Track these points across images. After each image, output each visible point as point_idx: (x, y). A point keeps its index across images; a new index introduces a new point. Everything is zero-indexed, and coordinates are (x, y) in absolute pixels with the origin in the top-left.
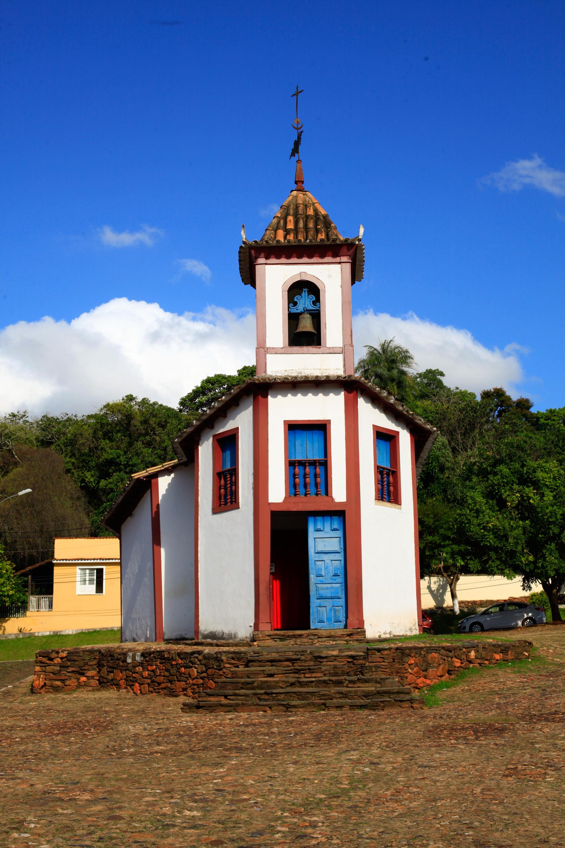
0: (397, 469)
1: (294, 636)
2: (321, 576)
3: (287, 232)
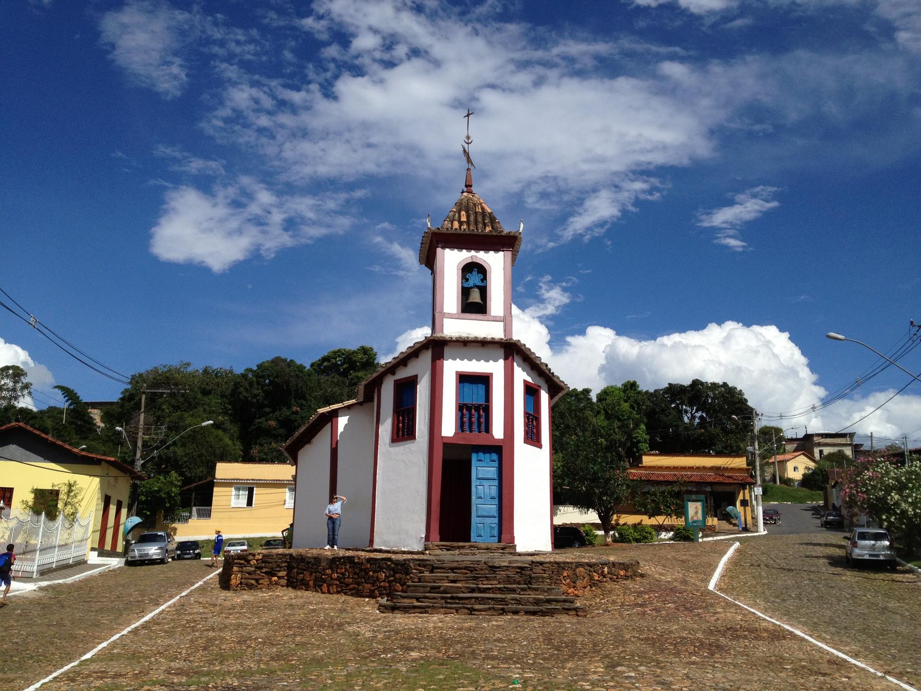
1: (459, 548)
2: (481, 498)
3: (461, 223)
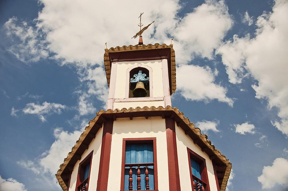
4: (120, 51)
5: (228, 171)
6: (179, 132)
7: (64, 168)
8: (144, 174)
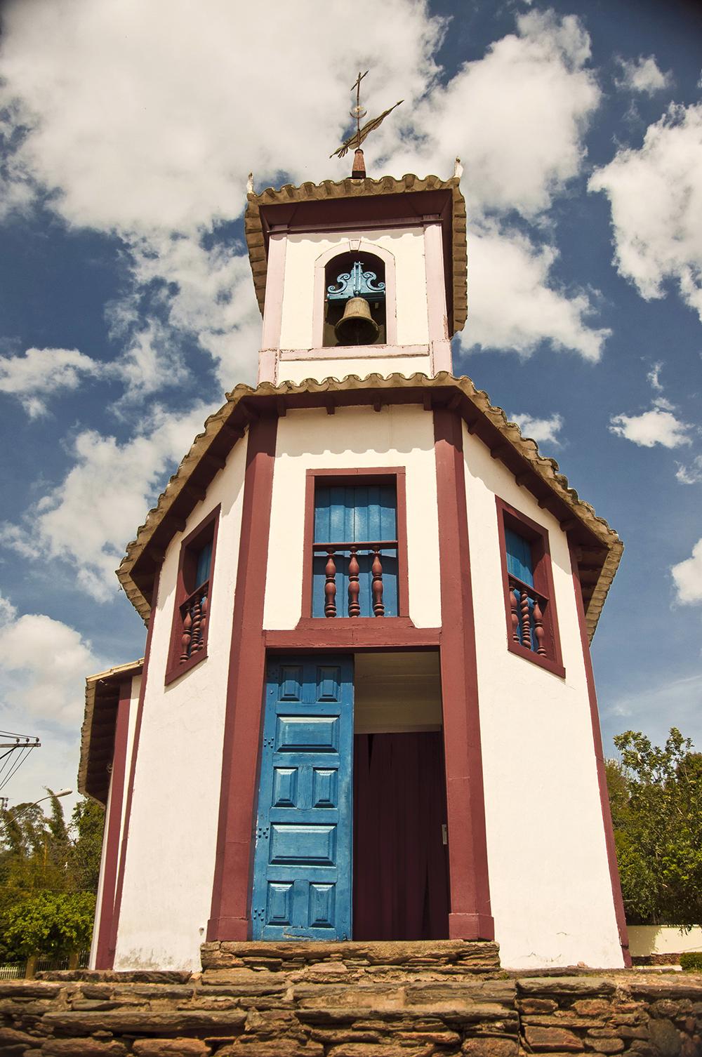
0: (548, 596)
4: (295, 201)
5: (611, 563)
6: (472, 448)
7: (138, 553)
8: (368, 572)
